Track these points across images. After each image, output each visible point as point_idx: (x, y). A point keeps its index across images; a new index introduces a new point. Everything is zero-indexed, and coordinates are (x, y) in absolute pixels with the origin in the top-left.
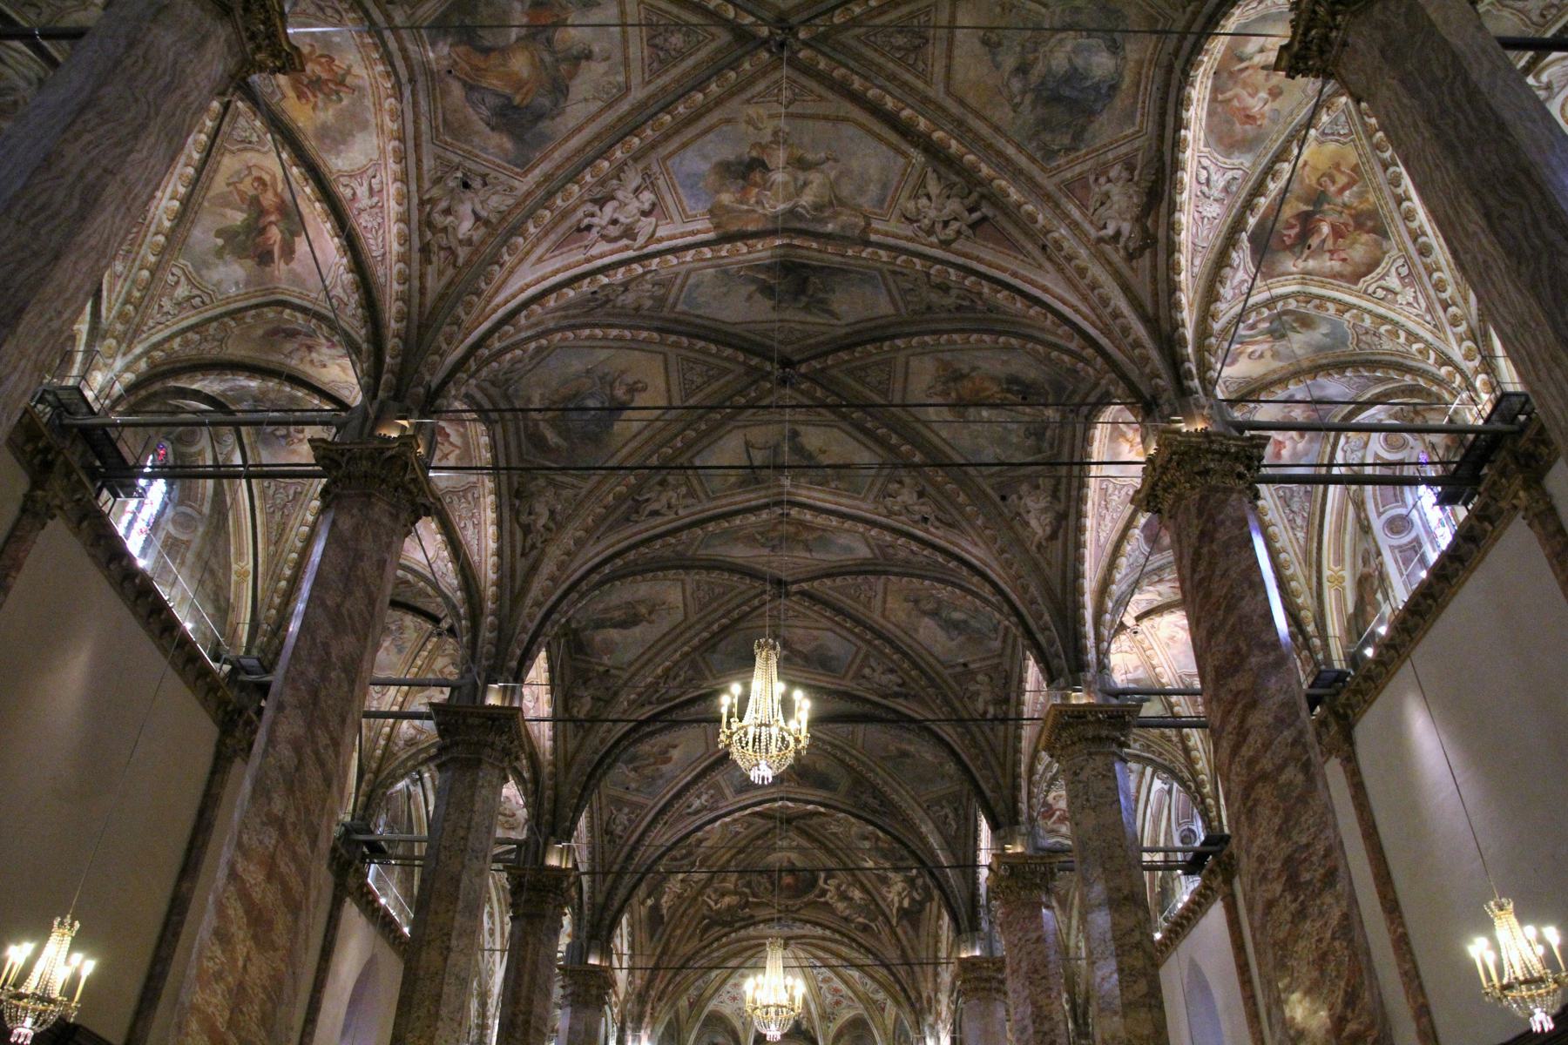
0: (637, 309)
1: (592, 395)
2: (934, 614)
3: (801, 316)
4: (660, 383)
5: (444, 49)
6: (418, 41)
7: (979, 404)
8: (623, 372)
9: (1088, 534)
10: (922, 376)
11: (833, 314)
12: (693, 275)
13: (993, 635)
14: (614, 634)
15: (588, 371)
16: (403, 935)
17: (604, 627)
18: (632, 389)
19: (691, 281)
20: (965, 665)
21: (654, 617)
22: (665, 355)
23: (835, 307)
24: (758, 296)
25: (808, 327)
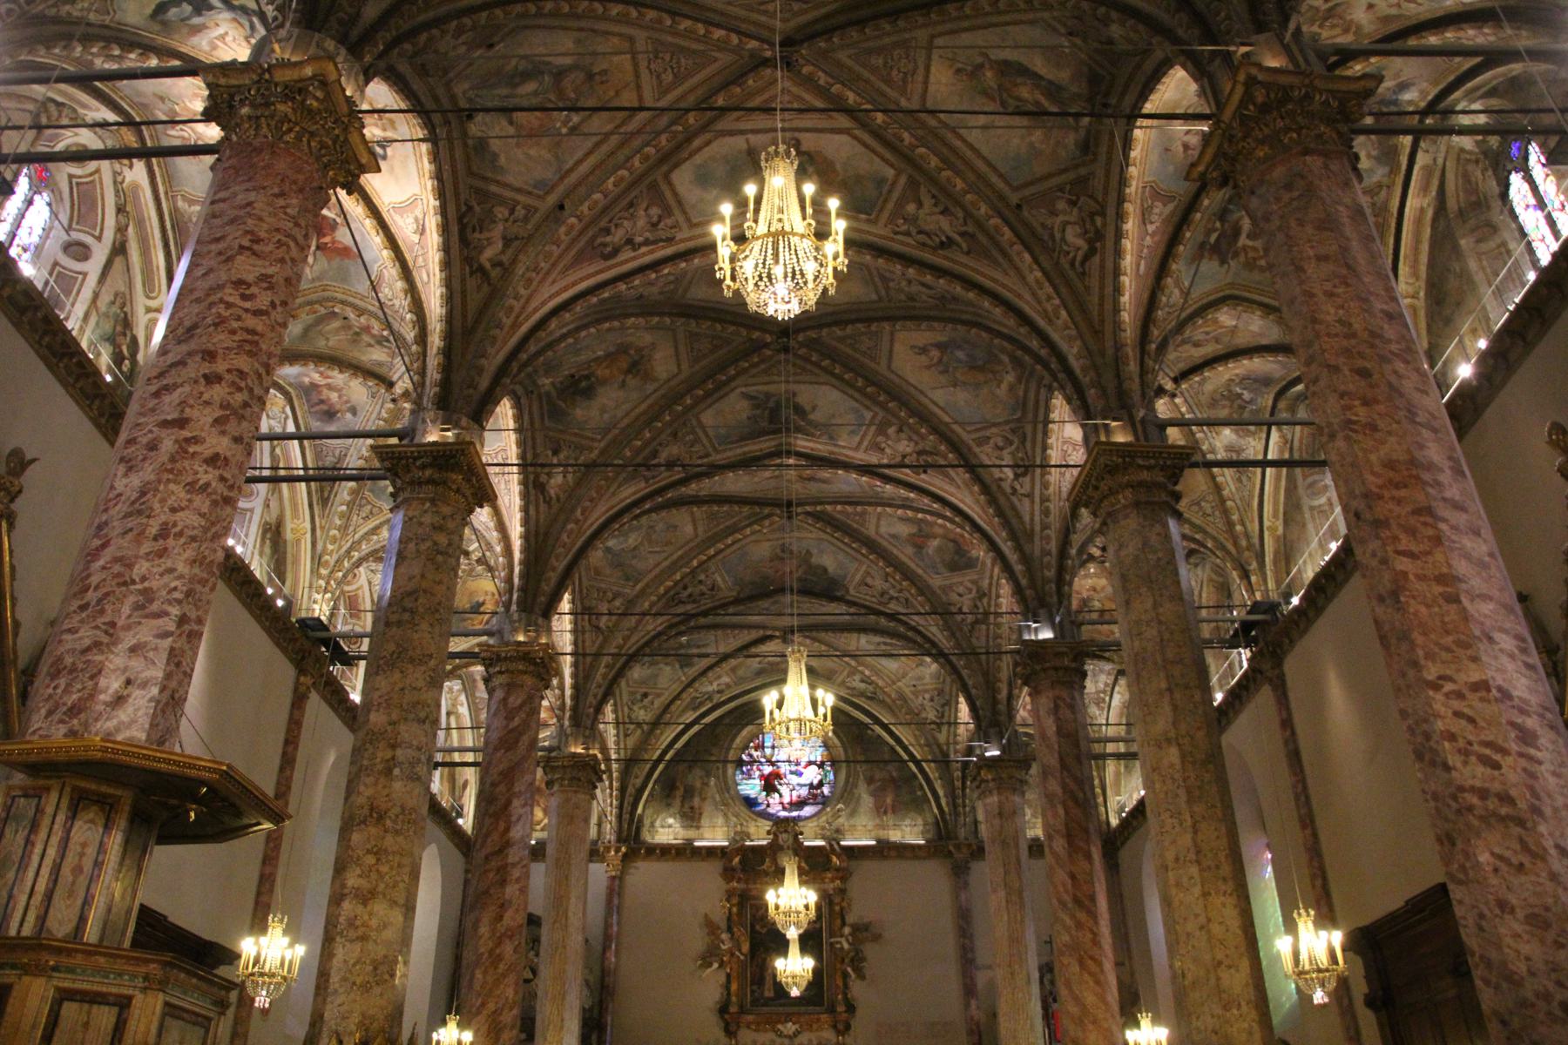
0: (900, 430)
1: (960, 361)
2: (560, 74)
3: (772, 388)
4: (897, 347)
5: (974, 553)
6: (984, 563)
7: (608, 355)
8: (928, 367)
9: (437, 259)
10: (664, 364)
11: (746, 396)
12: (854, 445)
13: (471, 94)
14: (1038, 64)
15: (955, 386)
16: (1211, 699)
17: (1050, 82)
18: (923, 350)
19: (857, 439)
20: (491, 46)
21: (979, 60)
22: (889, 367)
23: (745, 404)
24: (808, 408)
25: (767, 379)
